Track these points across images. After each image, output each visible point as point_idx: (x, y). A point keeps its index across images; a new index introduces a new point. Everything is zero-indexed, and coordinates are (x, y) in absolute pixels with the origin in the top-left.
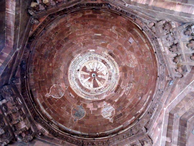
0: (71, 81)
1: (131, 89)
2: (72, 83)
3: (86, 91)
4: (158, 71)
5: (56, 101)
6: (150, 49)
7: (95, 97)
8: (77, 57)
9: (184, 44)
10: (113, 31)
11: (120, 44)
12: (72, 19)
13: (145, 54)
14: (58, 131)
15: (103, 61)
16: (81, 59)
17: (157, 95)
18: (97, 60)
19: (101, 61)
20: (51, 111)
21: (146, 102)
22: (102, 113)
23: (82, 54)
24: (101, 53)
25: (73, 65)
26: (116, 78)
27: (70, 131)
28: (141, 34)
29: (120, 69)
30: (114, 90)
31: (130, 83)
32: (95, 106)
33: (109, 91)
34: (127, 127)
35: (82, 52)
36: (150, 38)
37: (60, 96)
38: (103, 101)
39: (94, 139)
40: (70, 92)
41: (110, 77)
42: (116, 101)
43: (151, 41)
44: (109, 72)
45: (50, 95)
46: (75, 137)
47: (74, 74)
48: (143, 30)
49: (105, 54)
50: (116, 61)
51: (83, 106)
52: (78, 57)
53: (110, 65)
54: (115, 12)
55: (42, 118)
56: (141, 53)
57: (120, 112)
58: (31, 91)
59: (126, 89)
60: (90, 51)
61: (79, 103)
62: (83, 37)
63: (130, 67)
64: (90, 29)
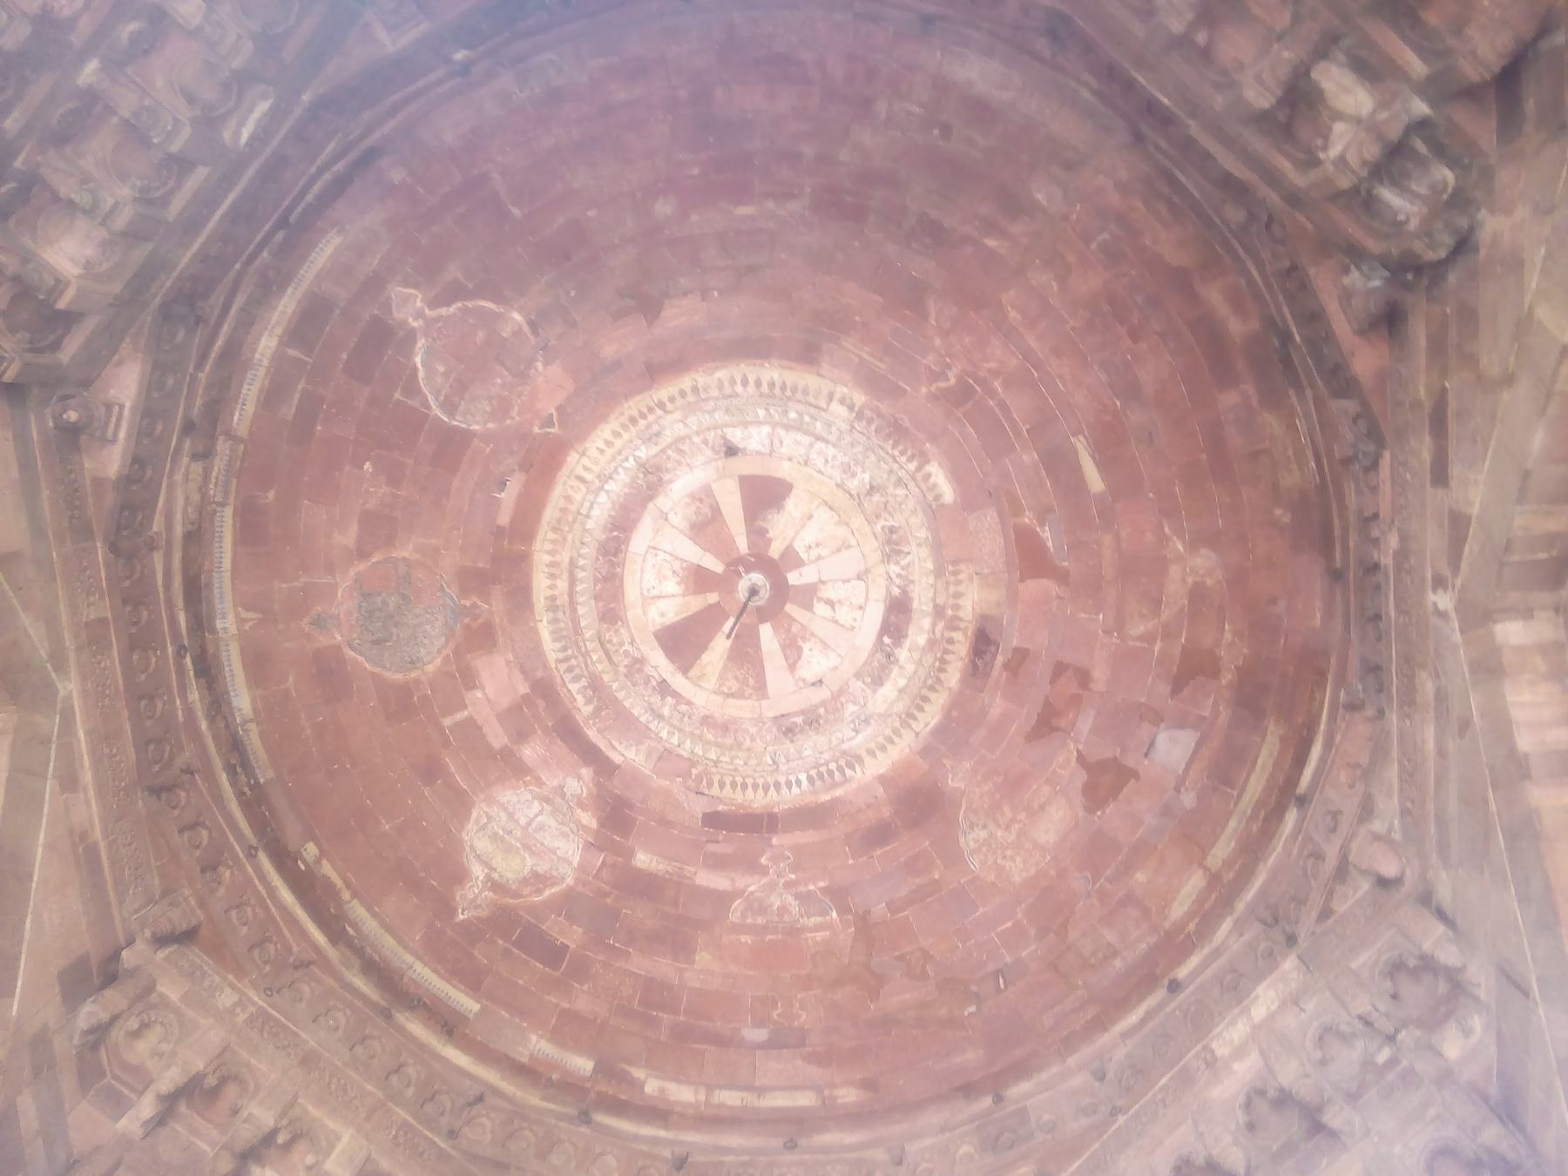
0: (616, 434)
1: (794, 931)
2: (610, 452)
3: (597, 597)
4: (1044, 1076)
5: (397, 395)
6: (1179, 927)
7: (584, 682)
8: (826, 386)
10: (1174, 572)
11: (1100, 675)
12: (1114, 198)
14: (169, 543)
15: (898, 611)
16: (829, 425)
17: (854, 1155)
18: (887, 558)
19: (896, 591)
20: (297, 395)
21: (751, 1100)
22: (490, 801)
23: (868, 413)
24: (955, 562)
25: (751, 388)
26: (821, 777)
27: (213, 630)
28: (1259, 804)
30: (720, 800)
31: (838, 896)
32: (518, 719)
33: (692, 763)
34: (483, 1053)
36: (1263, 892)
37: (450, 407)
38: (587, 763)
39: (251, 853)
40: (525, 466)
41: (799, 720)
42: (643, 859)
44: (841, 692)
45: (415, 324)
46: (194, 696)
47: (680, 430)
49: (958, 595)
50: (956, 703)
51: (467, 627)
52: (831, 397)
53: (897, 680)
54: (1336, 522)
55: (203, 358)
57: (572, 936)
58: (370, 157)
59: (772, 893)
61: (475, 581)
62: (1013, 362)
63: (962, 840)
64: (1104, 377)
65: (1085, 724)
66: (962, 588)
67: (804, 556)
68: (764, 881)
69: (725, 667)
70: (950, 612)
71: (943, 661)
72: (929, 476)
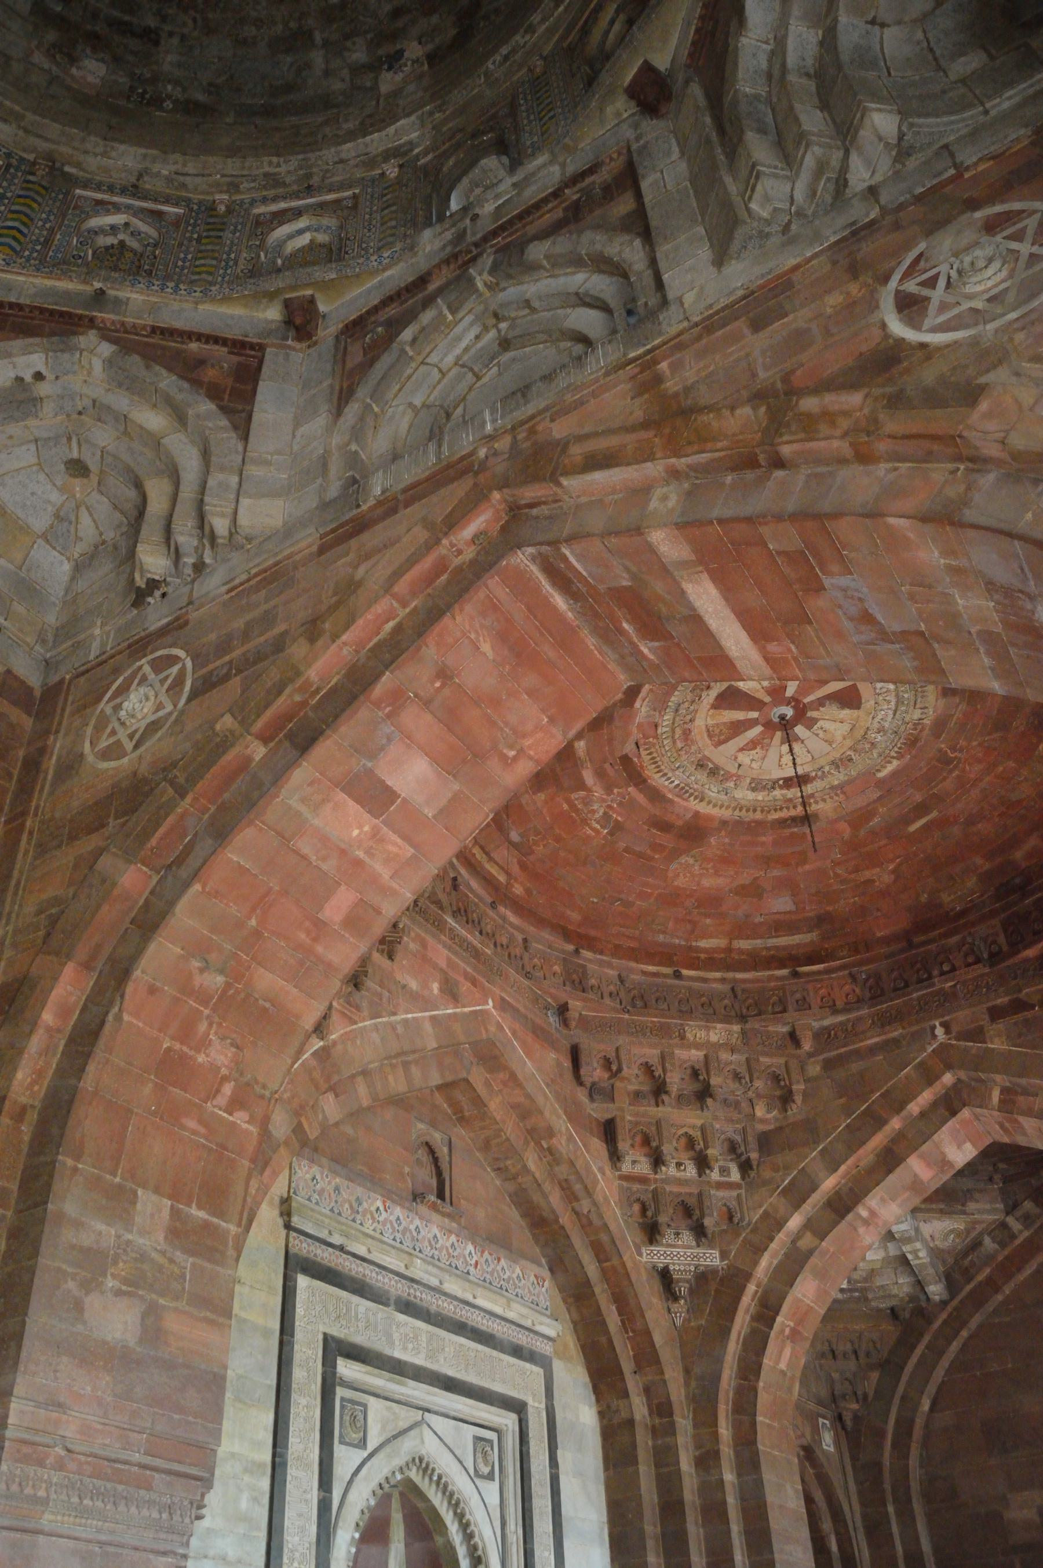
1: (585, 822)
6: (698, 950)
9: (694, 1127)
11: (807, 867)
13: (690, 921)
16: (906, 712)
24: (844, 793)
29: (710, 818)
30: (639, 756)
33: (656, 737)
35: (926, 732)
43: (735, 980)
48: (795, 974)
49: (824, 800)
50: (759, 823)
53: (760, 796)
60: (895, 763)
65: (776, 873)
71: (781, 809)
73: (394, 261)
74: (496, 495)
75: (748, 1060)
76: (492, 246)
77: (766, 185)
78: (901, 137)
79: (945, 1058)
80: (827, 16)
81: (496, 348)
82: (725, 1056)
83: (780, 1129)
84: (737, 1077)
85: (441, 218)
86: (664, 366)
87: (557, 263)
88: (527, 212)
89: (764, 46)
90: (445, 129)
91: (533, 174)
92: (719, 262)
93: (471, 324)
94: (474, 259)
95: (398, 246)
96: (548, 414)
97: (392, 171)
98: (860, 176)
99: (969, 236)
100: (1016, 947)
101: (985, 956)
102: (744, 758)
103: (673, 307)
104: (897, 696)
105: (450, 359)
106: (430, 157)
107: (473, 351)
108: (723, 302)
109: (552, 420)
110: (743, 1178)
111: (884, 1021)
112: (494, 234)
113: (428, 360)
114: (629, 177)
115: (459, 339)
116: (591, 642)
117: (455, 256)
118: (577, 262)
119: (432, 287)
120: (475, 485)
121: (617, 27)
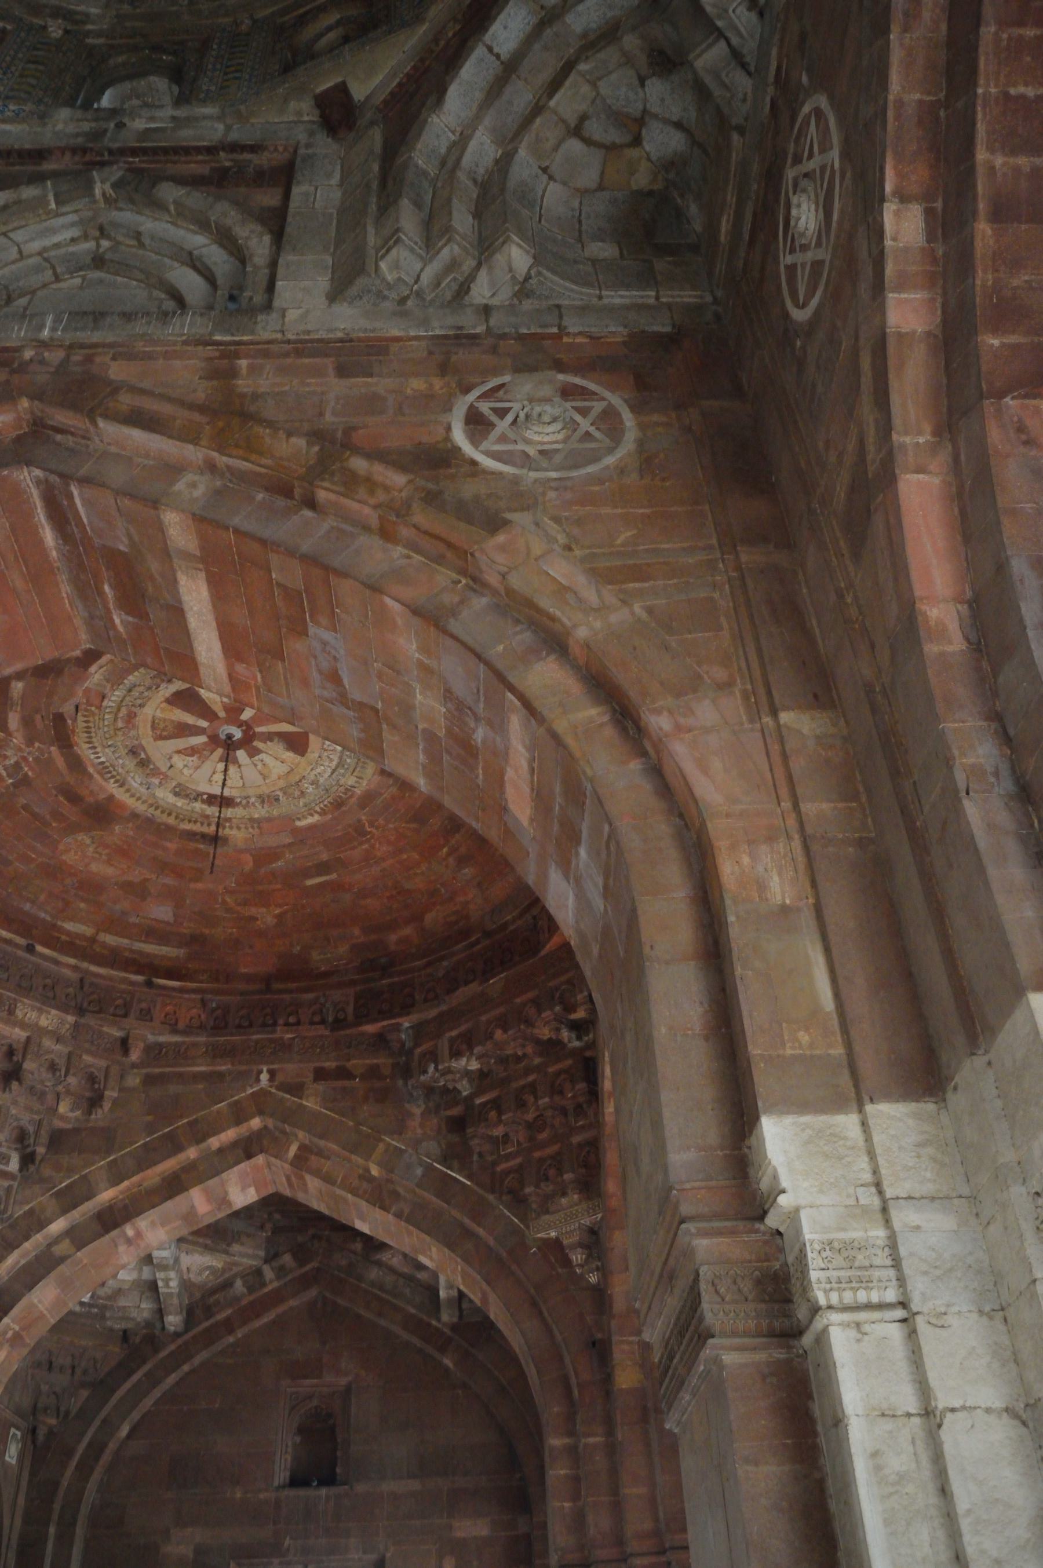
6: (61, 930)
10: (264, 910)
11: (200, 886)
12: (461, 899)
16: (343, 775)
24: (259, 828)
29: (122, 806)
30: (75, 720)
33: (99, 707)
35: (354, 800)
41: (143, 756)
43: (87, 972)
48: (149, 984)
49: (239, 828)
50: (169, 828)
53: (180, 803)
56: (81, 893)
60: (317, 817)
66: (243, 830)
67: (256, 758)
68: (23, 746)
69: (172, 721)
70: (227, 824)
71: (195, 822)
72: (312, 815)
73: (16, 118)
74: (25, 403)
75: (70, 1054)
76: (126, 162)
77: (399, 253)
78: (528, 278)
79: (260, 1103)
80: (512, 140)
81: (88, 260)
82: (47, 1043)
83: (76, 1131)
84: (53, 1067)
85: (87, 106)
86: (243, 363)
87: (182, 213)
88: (176, 150)
89: (450, 134)
90: (128, 24)
91: (196, 119)
92: (334, 296)
93: (73, 224)
94: (102, 164)
95: (28, 107)
96: (112, 351)
97: (55, 30)
98: (481, 291)
99: (546, 391)
100: (361, 1017)
101: (331, 1019)
102: (178, 761)
103: (274, 315)
104: (341, 758)
105: (36, 246)
106: (101, 41)
107: (62, 251)
108: (322, 335)
109: (114, 359)
110: (21, 1170)
111: (217, 1053)
112: (134, 152)
113: (11, 235)
114: (284, 176)
115: (54, 231)
116: (66, 589)
117: (84, 151)
118: (203, 225)
119: (48, 166)
120: (8, 381)
121: (332, 36)
